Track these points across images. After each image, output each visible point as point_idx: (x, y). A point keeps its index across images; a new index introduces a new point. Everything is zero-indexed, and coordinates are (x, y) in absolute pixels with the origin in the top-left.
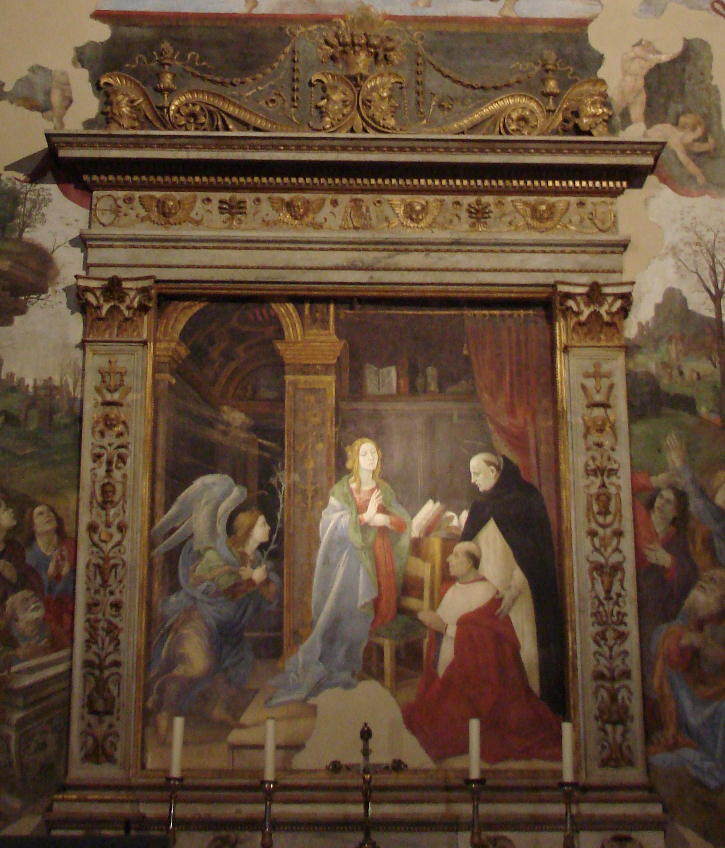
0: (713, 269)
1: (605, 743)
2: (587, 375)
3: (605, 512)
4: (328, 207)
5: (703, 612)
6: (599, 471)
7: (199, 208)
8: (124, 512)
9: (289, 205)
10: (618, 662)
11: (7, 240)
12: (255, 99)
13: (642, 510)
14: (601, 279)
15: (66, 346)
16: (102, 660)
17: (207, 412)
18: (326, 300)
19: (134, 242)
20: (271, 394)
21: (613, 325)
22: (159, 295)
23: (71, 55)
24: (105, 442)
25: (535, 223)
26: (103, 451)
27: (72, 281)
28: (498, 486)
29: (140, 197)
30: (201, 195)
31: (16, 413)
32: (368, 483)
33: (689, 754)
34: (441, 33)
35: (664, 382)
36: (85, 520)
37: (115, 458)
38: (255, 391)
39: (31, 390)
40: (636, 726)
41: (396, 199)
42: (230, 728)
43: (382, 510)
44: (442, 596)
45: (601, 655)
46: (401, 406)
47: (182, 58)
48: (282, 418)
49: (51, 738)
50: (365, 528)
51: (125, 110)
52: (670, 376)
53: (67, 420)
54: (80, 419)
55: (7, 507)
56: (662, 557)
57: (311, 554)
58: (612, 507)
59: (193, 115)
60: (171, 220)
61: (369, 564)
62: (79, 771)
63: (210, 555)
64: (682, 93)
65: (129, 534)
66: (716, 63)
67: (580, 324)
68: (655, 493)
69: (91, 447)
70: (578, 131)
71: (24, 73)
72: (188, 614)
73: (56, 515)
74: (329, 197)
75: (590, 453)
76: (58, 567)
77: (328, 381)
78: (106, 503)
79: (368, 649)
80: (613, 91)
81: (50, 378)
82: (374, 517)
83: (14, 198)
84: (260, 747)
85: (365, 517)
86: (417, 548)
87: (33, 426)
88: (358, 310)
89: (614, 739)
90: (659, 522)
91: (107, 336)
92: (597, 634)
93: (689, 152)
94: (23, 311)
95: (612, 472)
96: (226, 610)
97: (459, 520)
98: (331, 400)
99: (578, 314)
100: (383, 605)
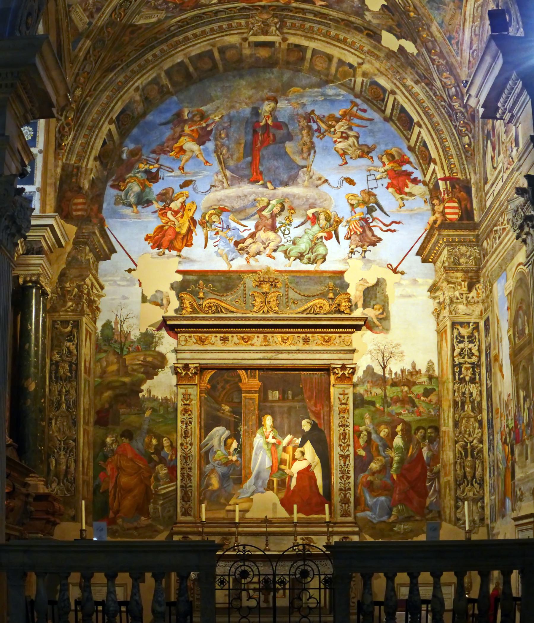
0: (383, 358)
2: (340, 394)
3: (345, 439)
4: (256, 338)
5: (375, 470)
7: (213, 340)
9: (243, 338)
11: (151, 351)
12: (231, 301)
13: (356, 438)
14: (345, 362)
15: (171, 386)
16: (186, 485)
17: (217, 406)
18: (255, 369)
19: (192, 351)
20: (236, 400)
21: (350, 378)
22: (201, 368)
23: (169, 286)
24: (185, 417)
25: (324, 343)
30: (214, 335)
32: (269, 429)
33: (368, 513)
34: (294, 276)
35: (366, 396)
36: (179, 442)
38: (232, 399)
42: (226, 505)
43: (274, 438)
44: (292, 465)
46: (280, 404)
47: (207, 286)
48: (241, 408)
49: (171, 509)
50: (268, 443)
51: (189, 306)
54: (176, 410)
56: (362, 453)
57: (251, 452)
59: (210, 307)
61: (269, 455)
62: (181, 518)
63: (219, 452)
64: (376, 297)
66: (387, 287)
67: (338, 377)
68: (361, 432)
71: (154, 293)
72: (213, 471)
74: (256, 335)
76: (171, 457)
77: (256, 395)
78: (186, 437)
82: (271, 440)
83: (152, 336)
84: (234, 511)
85: (268, 440)
86: (285, 449)
87: (162, 412)
90: (362, 442)
93: (377, 318)
94: (157, 374)
95: (347, 426)
96: (224, 469)
97: (298, 441)
98: (257, 402)
99: (337, 374)
100: (274, 468)
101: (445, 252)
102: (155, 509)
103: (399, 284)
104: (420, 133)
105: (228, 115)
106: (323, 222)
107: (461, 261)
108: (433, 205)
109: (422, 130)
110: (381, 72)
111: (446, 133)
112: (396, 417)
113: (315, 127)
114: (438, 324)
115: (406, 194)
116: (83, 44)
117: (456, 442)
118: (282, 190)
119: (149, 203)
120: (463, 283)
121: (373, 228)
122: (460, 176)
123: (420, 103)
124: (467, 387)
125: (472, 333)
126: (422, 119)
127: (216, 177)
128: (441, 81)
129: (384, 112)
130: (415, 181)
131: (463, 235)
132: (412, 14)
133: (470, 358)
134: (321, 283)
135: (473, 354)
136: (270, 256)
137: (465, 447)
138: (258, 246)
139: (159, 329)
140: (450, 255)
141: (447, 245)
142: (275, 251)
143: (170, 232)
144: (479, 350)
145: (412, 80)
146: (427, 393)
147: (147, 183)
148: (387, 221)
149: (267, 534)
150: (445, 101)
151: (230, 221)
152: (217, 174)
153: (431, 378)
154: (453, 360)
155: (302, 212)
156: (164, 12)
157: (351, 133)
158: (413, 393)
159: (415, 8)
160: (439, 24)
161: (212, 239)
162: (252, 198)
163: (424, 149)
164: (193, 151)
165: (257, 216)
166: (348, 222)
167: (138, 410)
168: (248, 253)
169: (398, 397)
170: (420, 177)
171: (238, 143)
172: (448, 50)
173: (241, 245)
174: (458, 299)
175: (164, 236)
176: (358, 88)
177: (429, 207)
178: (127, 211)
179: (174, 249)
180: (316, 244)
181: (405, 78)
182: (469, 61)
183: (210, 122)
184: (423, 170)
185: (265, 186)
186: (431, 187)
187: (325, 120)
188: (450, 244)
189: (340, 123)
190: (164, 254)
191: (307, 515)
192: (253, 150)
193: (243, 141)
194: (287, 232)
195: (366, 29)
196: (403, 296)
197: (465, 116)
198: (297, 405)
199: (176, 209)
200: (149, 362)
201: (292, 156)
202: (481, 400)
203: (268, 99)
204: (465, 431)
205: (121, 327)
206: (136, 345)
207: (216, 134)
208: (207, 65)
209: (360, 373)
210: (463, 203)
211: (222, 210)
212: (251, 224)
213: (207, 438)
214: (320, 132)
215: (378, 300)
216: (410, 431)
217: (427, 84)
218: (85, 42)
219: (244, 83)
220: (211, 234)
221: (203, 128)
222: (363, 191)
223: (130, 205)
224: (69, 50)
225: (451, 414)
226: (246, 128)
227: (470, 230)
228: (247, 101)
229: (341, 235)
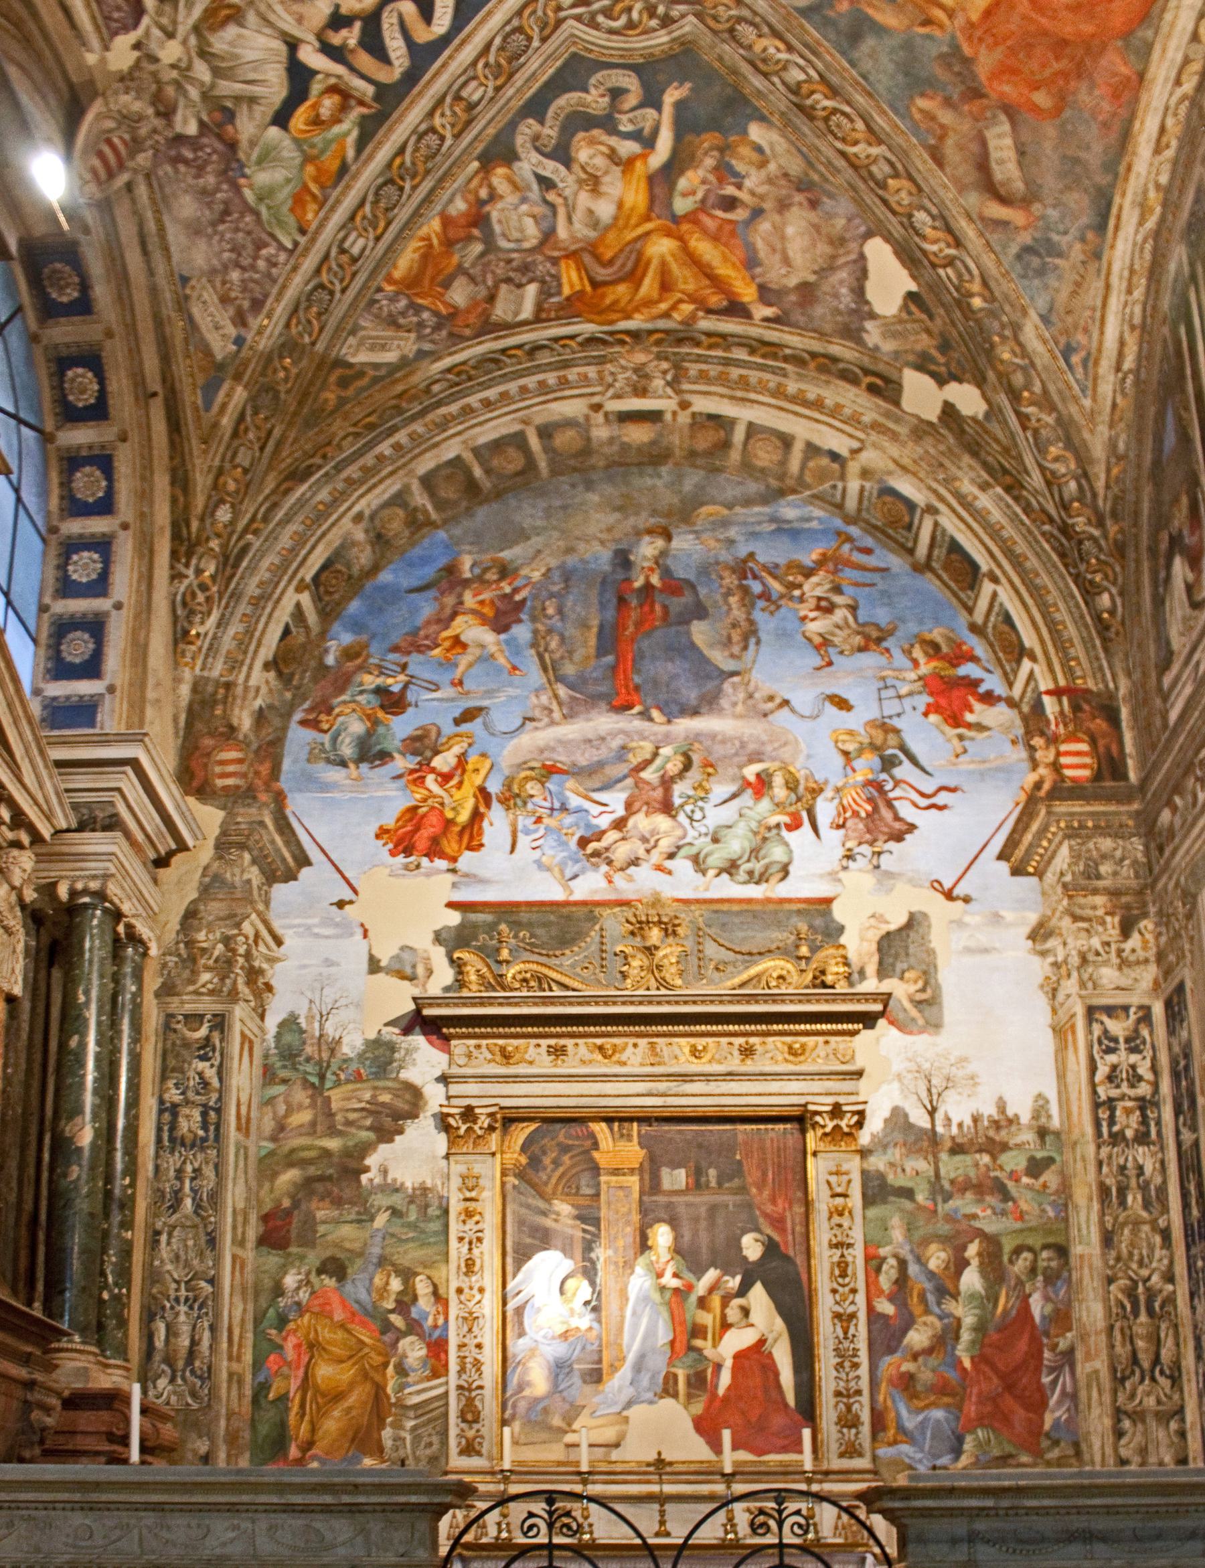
3: (844, 1275)
4: (630, 1049)
7: (532, 1053)
9: (601, 1048)
12: (573, 966)
14: (841, 1100)
18: (631, 1120)
19: (482, 1078)
23: (431, 936)
27: (437, 1109)
28: (763, 1256)
30: (534, 1041)
32: (665, 1256)
33: (905, 1448)
36: (453, 1286)
41: (683, 1041)
43: (675, 1275)
46: (689, 1198)
50: (663, 1289)
51: (473, 977)
54: (446, 1212)
56: (886, 1307)
59: (525, 980)
61: (665, 1315)
68: (884, 1259)
70: (824, 985)
71: (395, 951)
74: (631, 1041)
77: (633, 1181)
79: (666, 1378)
80: (852, 955)
82: (669, 1281)
83: (392, 1047)
85: (663, 1281)
86: (702, 1303)
88: (655, 1128)
90: (885, 1281)
93: (912, 1001)
94: (401, 1132)
95: (849, 1246)
96: (559, 1350)
97: (734, 1282)
98: (636, 1195)
100: (677, 1345)
101: (1064, 851)
102: (397, 1439)
103: (960, 924)
104: (995, 595)
105: (562, 567)
106: (780, 792)
107: (1104, 869)
108: (1032, 749)
109: (999, 589)
110: (904, 468)
111: (1054, 593)
113: (757, 587)
114: (1054, 1011)
115: (969, 726)
116: (229, 395)
117: (1110, 1280)
118: (685, 725)
119: (384, 756)
120: (1108, 919)
121: (896, 803)
122: (1091, 684)
123: (994, 532)
124: (1130, 1153)
125: (1136, 1031)
126: (999, 566)
127: (534, 700)
128: (1042, 469)
129: (911, 552)
130: (989, 698)
131: (1104, 813)
132: (977, 302)
133: (1132, 1086)
134: (779, 925)
135: (1140, 1079)
136: (659, 868)
137: (1131, 1293)
138: (633, 847)
139: (407, 1031)
140: (1076, 856)
141: (1068, 837)
142: (671, 856)
143: (434, 819)
144: (1154, 1069)
145: (973, 481)
146: (1036, 1167)
147: (381, 714)
148: (928, 786)
149: (662, 1499)
150: (1051, 520)
151: (568, 794)
152: (537, 692)
153: (1042, 1133)
154: (1095, 1092)
155: (732, 771)
156: (413, 336)
157: (838, 599)
158: (1001, 1168)
159: (985, 284)
160: (1041, 316)
161: (527, 832)
162: (615, 743)
163: (1006, 629)
164: (483, 646)
165: (629, 781)
166: (838, 790)
168: (610, 863)
169: (968, 1178)
170: (1000, 689)
171: (585, 626)
172: (1061, 385)
173: (593, 846)
174: (1098, 954)
175: (417, 829)
176: (851, 504)
177: (1024, 754)
178: (335, 775)
179: (442, 855)
180: (765, 839)
181: (956, 479)
182: (1114, 405)
183: (518, 583)
184: (1005, 674)
185: (645, 715)
186: (1026, 709)
187: (779, 572)
188: (1071, 833)
189: (814, 579)
190: (418, 866)
192: (616, 640)
193: (595, 623)
194: (698, 815)
195: (867, 372)
196: (968, 950)
197: (1101, 549)
198: (729, 1199)
199: (445, 769)
200: (383, 1104)
201: (707, 652)
202: (1165, 1182)
203: (650, 532)
204: (1131, 1254)
205: (321, 1028)
206: (354, 1066)
207: (533, 608)
208: (512, 462)
209: (875, 1124)
210: (1101, 743)
211: (551, 770)
212: (616, 800)
213: (520, 1276)
214: (768, 599)
215: (912, 960)
217: (1008, 489)
218: (232, 389)
219: (594, 498)
220: (524, 821)
221: (505, 596)
222: (872, 724)
223: (343, 764)
224: (197, 409)
225: (1094, 1217)
226: (601, 594)
227: (1119, 802)
228: (604, 536)
229: (824, 818)
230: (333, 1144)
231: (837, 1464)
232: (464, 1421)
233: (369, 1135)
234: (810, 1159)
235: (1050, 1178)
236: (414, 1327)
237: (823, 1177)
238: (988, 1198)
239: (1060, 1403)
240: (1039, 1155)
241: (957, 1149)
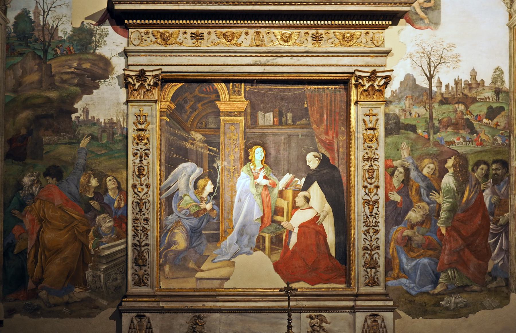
1: (367, 276)
6: (368, 159)
8: (149, 179)
10: (374, 242)
15: (118, 103)
26: (138, 152)
29: (152, 32)
31: (96, 135)
37: (144, 155)
39: (103, 124)
40: (381, 269)
45: (367, 239)
52: (405, 115)
53: (121, 138)
54: (127, 137)
55: (94, 178)
58: (375, 176)
60: (168, 43)
65: (151, 189)
69: (132, 150)
73: (117, 180)
75: (366, 151)
81: (112, 119)
89: (371, 275)
91: (138, 98)
92: (366, 231)
95: (376, 159)
112: (446, 147)
167: (70, 138)
191: (313, 285)
216: (467, 168)
230: (53, 95)
231: (363, 290)
232: (137, 265)
233: (78, 89)
234: (353, 107)
235: (501, 119)
236: (106, 208)
237: (361, 117)
238: (461, 132)
239: (498, 255)
240: (495, 105)
241: (444, 101)
